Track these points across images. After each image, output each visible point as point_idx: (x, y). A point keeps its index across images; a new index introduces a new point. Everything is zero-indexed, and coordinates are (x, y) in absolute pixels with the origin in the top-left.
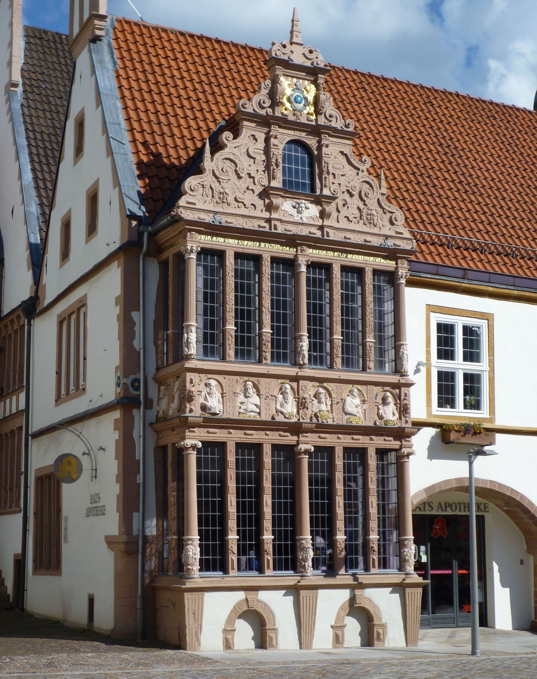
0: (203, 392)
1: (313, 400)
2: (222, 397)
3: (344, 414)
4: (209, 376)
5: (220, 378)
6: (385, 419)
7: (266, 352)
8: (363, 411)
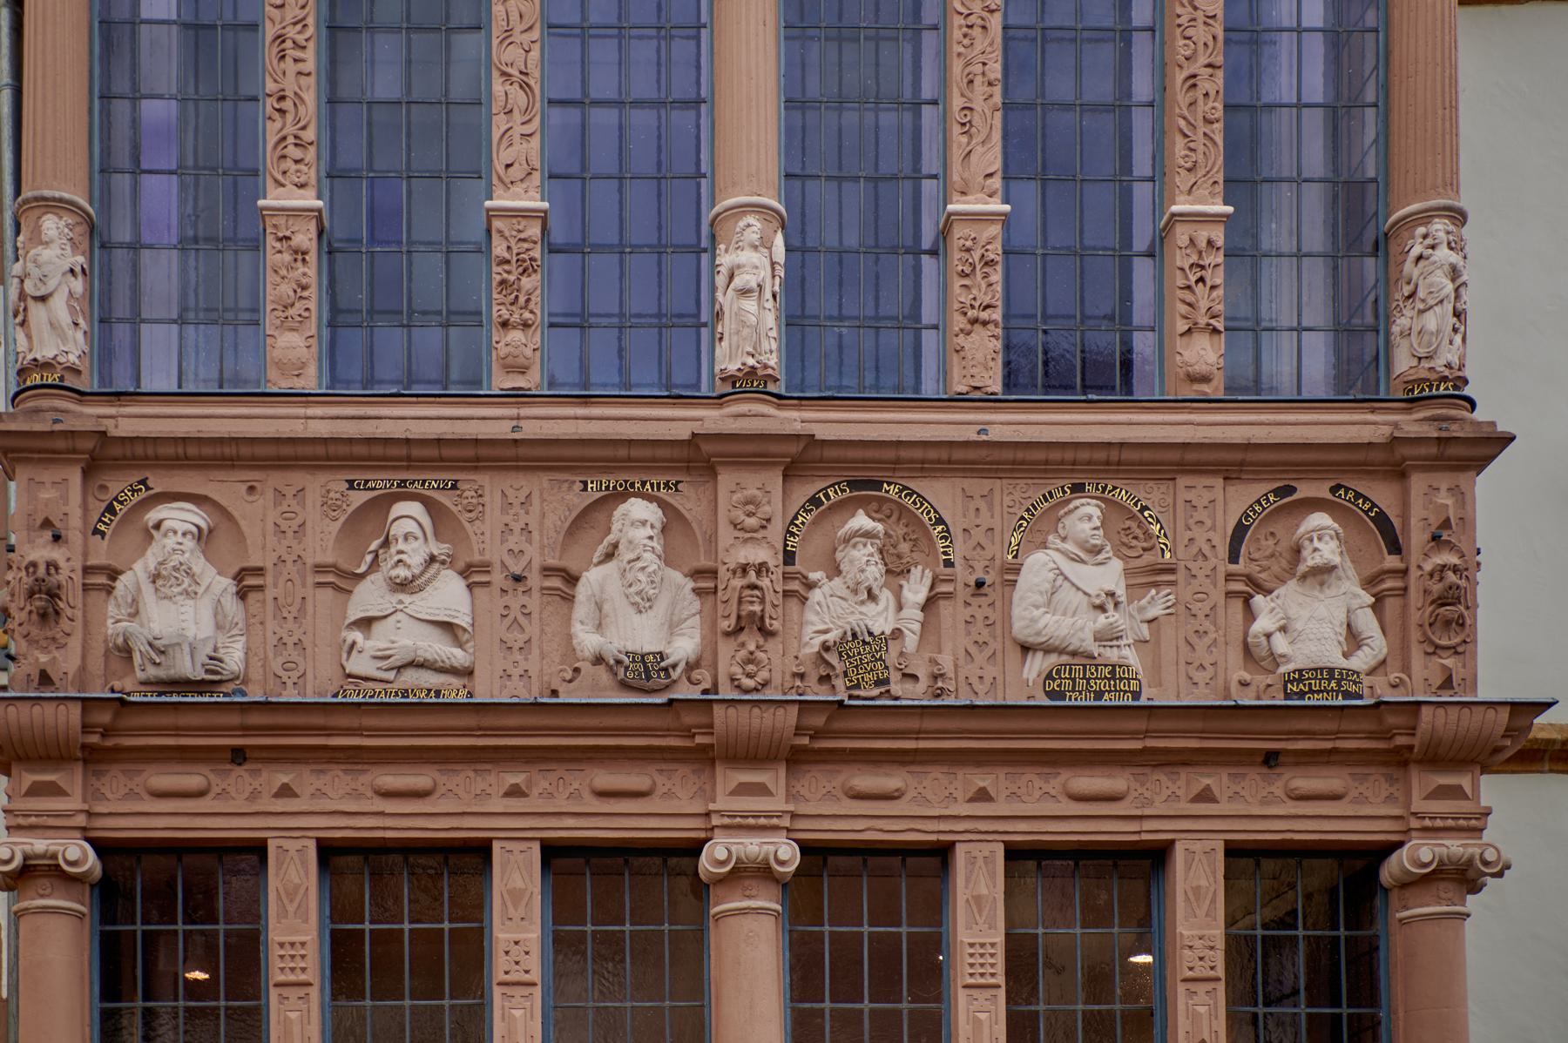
1: (810, 586)
2: (242, 594)
4: (159, 483)
5: (226, 488)
6: (1291, 667)
7: (505, 324)
8: (1145, 631)
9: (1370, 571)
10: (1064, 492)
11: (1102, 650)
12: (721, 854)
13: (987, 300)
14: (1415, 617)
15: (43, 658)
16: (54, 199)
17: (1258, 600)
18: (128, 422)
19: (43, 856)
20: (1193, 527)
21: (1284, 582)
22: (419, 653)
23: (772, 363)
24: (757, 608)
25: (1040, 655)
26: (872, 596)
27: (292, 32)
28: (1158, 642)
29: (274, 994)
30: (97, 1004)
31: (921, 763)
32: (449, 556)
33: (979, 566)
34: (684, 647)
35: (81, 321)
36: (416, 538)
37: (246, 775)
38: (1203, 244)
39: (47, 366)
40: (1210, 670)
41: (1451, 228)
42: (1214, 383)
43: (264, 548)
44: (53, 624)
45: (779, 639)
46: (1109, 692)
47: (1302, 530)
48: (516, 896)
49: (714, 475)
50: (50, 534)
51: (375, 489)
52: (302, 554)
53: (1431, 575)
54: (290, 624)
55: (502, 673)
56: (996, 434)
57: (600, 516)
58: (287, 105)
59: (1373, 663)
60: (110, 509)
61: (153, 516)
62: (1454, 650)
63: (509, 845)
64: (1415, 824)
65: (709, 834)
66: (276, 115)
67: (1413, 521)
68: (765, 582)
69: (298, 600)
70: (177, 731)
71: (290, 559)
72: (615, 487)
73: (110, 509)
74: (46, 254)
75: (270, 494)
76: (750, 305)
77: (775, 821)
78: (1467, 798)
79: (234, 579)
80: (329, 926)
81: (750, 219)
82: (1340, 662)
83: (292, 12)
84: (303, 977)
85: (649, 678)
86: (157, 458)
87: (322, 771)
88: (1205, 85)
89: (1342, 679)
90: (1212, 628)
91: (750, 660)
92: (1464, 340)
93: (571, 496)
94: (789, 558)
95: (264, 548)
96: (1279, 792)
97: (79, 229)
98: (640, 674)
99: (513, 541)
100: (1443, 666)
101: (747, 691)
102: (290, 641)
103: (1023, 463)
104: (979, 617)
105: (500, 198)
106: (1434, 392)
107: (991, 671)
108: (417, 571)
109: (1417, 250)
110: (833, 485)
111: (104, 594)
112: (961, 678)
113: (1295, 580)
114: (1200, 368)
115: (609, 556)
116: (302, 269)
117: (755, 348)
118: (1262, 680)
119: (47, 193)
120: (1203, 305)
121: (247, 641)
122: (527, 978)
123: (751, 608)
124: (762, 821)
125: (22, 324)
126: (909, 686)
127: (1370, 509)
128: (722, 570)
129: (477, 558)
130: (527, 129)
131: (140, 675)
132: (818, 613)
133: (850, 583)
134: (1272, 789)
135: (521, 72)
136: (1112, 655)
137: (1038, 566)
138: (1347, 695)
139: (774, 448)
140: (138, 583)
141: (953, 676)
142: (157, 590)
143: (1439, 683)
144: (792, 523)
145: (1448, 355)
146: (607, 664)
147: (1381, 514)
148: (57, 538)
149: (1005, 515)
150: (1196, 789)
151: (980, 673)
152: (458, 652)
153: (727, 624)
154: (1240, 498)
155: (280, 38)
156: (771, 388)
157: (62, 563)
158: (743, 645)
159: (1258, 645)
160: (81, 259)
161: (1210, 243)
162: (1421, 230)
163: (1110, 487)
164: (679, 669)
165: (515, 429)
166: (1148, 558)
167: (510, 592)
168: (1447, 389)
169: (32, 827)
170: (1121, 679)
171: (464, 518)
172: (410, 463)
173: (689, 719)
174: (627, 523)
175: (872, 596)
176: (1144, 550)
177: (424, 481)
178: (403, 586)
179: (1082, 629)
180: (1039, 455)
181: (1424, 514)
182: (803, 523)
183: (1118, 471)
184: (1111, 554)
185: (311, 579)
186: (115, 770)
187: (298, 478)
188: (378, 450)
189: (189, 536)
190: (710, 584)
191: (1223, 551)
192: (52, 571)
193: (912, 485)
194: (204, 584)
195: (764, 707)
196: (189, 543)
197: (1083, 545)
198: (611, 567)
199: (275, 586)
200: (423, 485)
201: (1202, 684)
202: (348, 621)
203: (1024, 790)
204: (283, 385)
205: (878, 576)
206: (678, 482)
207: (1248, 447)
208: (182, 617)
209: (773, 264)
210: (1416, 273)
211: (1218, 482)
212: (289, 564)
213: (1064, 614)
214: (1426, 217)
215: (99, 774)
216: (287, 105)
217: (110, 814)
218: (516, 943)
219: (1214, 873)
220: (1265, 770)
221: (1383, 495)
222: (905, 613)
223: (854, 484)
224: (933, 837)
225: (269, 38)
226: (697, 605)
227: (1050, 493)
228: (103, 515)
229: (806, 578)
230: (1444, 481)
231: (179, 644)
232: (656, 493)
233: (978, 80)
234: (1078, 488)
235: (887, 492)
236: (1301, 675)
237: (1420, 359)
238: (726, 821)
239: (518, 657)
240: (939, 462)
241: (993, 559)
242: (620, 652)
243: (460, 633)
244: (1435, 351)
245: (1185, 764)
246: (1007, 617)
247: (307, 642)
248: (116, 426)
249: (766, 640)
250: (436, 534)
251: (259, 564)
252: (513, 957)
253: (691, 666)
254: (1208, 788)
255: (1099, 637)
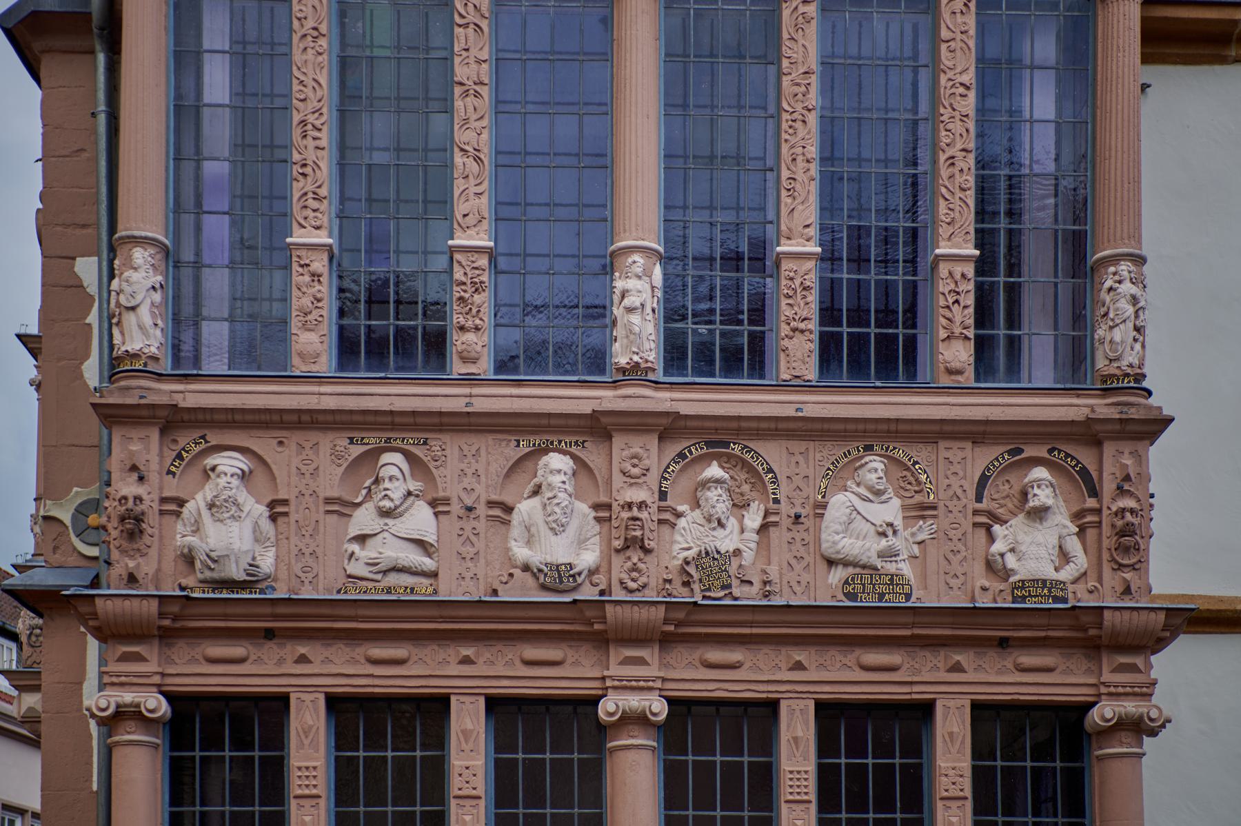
0: (190, 506)
1: (679, 515)
2: (273, 518)
3: (822, 566)
4: (214, 439)
5: (263, 444)
6: (1016, 578)
7: (462, 328)
8: (916, 550)
9: (1075, 508)
10: (859, 451)
11: (884, 564)
12: (611, 707)
13: (805, 314)
14: (1106, 543)
15: (131, 564)
16: (141, 237)
17: (997, 528)
18: (193, 396)
19: (130, 705)
20: (950, 476)
21: (1016, 515)
22: (399, 561)
23: (651, 358)
24: (638, 533)
25: (840, 567)
26: (721, 524)
27: (311, 118)
28: (925, 558)
29: (293, 803)
30: (167, 809)
31: (756, 643)
32: (421, 491)
33: (798, 502)
34: (588, 558)
35: (159, 322)
36: (398, 479)
37: (275, 647)
38: (958, 277)
39: (135, 356)
40: (962, 578)
41: (1132, 268)
42: (966, 374)
43: (289, 485)
44: (138, 539)
45: (654, 554)
46: (889, 593)
47: (1026, 480)
48: (466, 734)
49: (610, 437)
50: (137, 475)
51: (368, 444)
52: (316, 489)
53: (1116, 514)
54: (307, 540)
55: (458, 576)
56: (810, 411)
57: (529, 464)
58: (308, 170)
59: (1076, 574)
60: (179, 457)
61: (210, 461)
62: (1132, 567)
63: (462, 698)
64: (1103, 690)
65: (604, 692)
66: (300, 178)
67: (1106, 475)
68: (644, 515)
69: (313, 523)
70: (226, 617)
71: (307, 493)
72: (539, 444)
73: (179, 457)
74: (135, 276)
75: (294, 447)
76: (635, 319)
77: (651, 684)
78: (1141, 672)
79: (268, 506)
80: (334, 753)
81: (636, 257)
82: (1050, 573)
83: (312, 105)
84: (314, 791)
85: (561, 582)
86: (212, 421)
87: (329, 645)
88: (960, 164)
89: (1052, 587)
90: (964, 548)
91: (635, 569)
92: (1143, 346)
93: (506, 451)
94: (663, 495)
95: (289, 485)
96: (1010, 666)
97: (158, 256)
98: (555, 579)
99: (468, 482)
100: (1124, 579)
101: (631, 591)
102: (307, 552)
103: (829, 431)
104: (798, 540)
105: (459, 238)
106: (1120, 385)
107: (806, 577)
108: (397, 503)
109: (1108, 284)
110: (694, 444)
111: (174, 518)
112: (785, 582)
113: (1023, 515)
114: (955, 365)
115: (536, 491)
116: (318, 287)
117: (639, 348)
118: (998, 586)
119: (136, 233)
120: (958, 319)
121: (277, 551)
122: (474, 793)
123: (634, 533)
124: (642, 684)
125: (118, 324)
126: (746, 588)
127: (1076, 465)
128: (615, 505)
129: (441, 494)
130: (479, 189)
131: (200, 576)
132: (683, 536)
133: (706, 515)
134: (1006, 663)
135: (475, 149)
136: (891, 568)
137: (839, 503)
138: (1056, 599)
139: (650, 420)
140: (199, 510)
141: (778, 581)
142: (212, 515)
143: (1122, 590)
144: (665, 471)
145: (1131, 358)
146: (532, 572)
147: (1084, 468)
148: (141, 479)
149: (817, 467)
150: (950, 663)
151: (798, 579)
152: (427, 560)
153: (617, 544)
154: (981, 459)
155: (303, 123)
156: (651, 377)
157: (145, 497)
158: (629, 558)
159: (995, 561)
160: (160, 278)
161: (963, 276)
162: (1112, 269)
163: (891, 448)
164: (583, 576)
165: (467, 405)
166: (918, 498)
167: (465, 519)
168: (1129, 382)
169: (122, 684)
170: (897, 585)
171: (432, 465)
172: (394, 427)
173: (589, 613)
174: (547, 470)
175: (721, 524)
176: (916, 492)
177: (404, 439)
178: (386, 513)
179: (869, 550)
180: (841, 426)
181: (1113, 470)
182: (673, 471)
183: (896, 437)
184: (892, 495)
185: (322, 508)
186: (181, 643)
187: (314, 436)
188: (370, 418)
189: (236, 477)
190: (607, 514)
191: (972, 493)
192: (138, 503)
193: (751, 445)
194: (246, 509)
195: (641, 605)
196: (235, 482)
197: (871, 489)
198: (535, 502)
199: (297, 512)
200: (403, 441)
201: (955, 588)
202: (349, 537)
203: (829, 662)
204: (304, 369)
205: (725, 510)
206: (584, 441)
207: (987, 422)
208: (230, 535)
209: (653, 287)
210: (1108, 299)
211: (969, 445)
212: (307, 496)
213: (857, 538)
214: (1115, 259)
215: (169, 645)
216: (308, 170)
217: (178, 675)
218: (467, 768)
219: (963, 722)
220: (1000, 650)
221: (1086, 457)
222: (747, 535)
223: (709, 444)
224: (764, 695)
225: (295, 121)
226: (597, 528)
227: (849, 451)
228: (174, 461)
229: (675, 510)
230: (1127, 447)
231: (227, 556)
232: (569, 449)
233: (800, 158)
234: (869, 448)
235: (733, 449)
236: (1023, 584)
237: (1111, 360)
238: (616, 683)
239: (470, 564)
240: (769, 430)
241: (808, 498)
242: (541, 563)
243: (428, 547)
244: (1121, 355)
245: (944, 645)
246: (818, 541)
247: (319, 551)
248: (184, 399)
249: (645, 554)
250: (413, 475)
251: (286, 497)
252: (465, 778)
253: (592, 572)
254: (958, 662)
255: (881, 555)
